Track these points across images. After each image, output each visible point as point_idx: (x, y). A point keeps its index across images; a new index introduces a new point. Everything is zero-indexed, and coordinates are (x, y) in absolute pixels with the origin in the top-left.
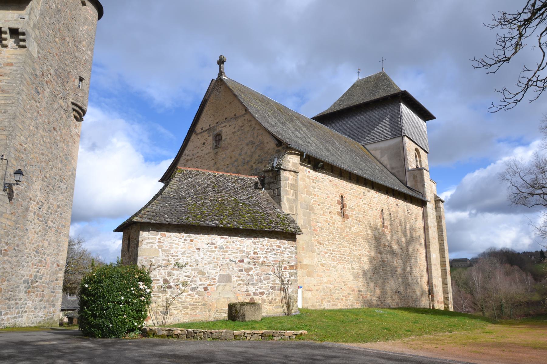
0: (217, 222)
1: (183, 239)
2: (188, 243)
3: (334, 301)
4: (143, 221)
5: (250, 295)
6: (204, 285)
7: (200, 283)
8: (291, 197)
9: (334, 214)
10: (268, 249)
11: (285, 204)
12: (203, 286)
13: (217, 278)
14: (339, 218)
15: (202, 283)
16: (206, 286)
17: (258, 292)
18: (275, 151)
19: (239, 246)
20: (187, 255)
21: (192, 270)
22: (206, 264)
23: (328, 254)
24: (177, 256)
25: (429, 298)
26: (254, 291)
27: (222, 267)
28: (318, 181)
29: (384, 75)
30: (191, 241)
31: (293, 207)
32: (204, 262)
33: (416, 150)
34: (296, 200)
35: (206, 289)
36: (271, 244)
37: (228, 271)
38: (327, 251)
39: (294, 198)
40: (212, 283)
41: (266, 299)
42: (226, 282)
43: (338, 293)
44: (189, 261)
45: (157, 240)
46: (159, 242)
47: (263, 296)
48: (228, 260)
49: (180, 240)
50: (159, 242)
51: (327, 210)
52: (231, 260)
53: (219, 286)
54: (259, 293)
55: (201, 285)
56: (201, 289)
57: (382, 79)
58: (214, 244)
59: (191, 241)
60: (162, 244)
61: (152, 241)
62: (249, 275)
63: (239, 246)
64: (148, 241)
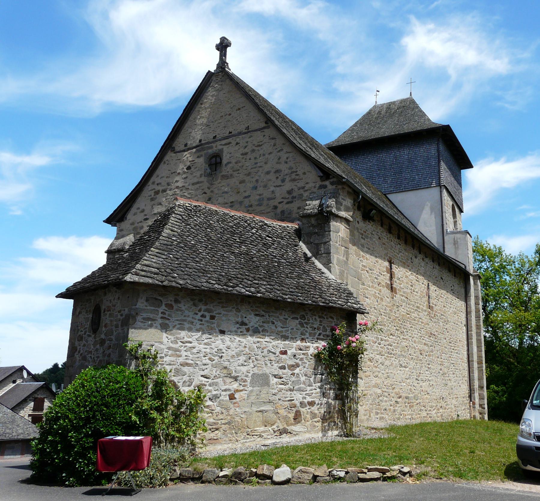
0: (253, 289)
1: (200, 314)
2: (207, 321)
3: (382, 413)
4: (141, 281)
5: (295, 406)
6: (229, 390)
7: (224, 388)
8: (341, 258)
9: (383, 286)
10: (320, 334)
11: (335, 267)
12: (228, 393)
13: (249, 380)
14: (386, 292)
15: (227, 387)
16: (232, 392)
17: (306, 401)
18: (318, 186)
19: (280, 329)
20: (206, 341)
21: (212, 366)
22: (233, 356)
23: (377, 344)
24: (191, 343)
25: (470, 406)
26: (301, 400)
27: (256, 363)
28: (367, 237)
29: (412, 102)
30: (212, 318)
31: (344, 271)
32: (231, 353)
33: (453, 205)
34: (346, 263)
35: (232, 397)
36: (324, 327)
37: (265, 369)
38: (375, 340)
39: (345, 259)
40: (242, 388)
41: (316, 412)
42: (262, 385)
43: (386, 401)
44: (208, 351)
45: (160, 315)
46: (162, 318)
47: (313, 408)
48: (265, 350)
49: (195, 316)
50: (162, 318)
51: (376, 280)
52: (270, 351)
53: (251, 391)
54: (308, 403)
55: (225, 390)
56: (225, 397)
57: (408, 107)
58: (246, 324)
59: (212, 318)
60: (167, 322)
61: (151, 316)
62: (293, 374)
63: (280, 329)
64: (145, 315)
